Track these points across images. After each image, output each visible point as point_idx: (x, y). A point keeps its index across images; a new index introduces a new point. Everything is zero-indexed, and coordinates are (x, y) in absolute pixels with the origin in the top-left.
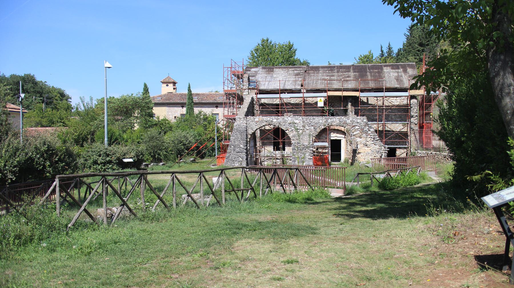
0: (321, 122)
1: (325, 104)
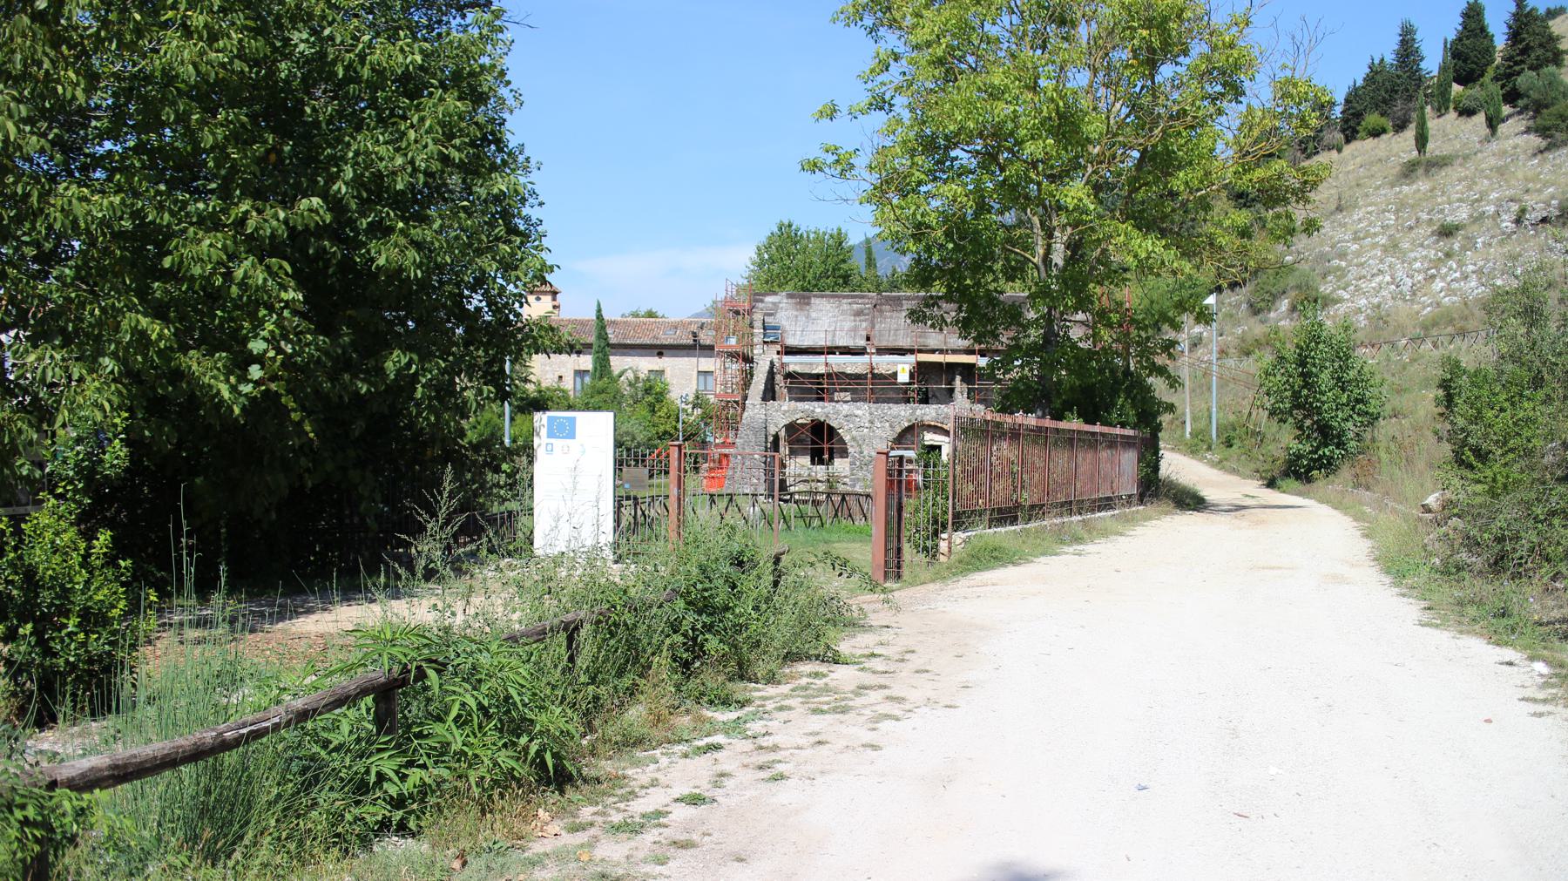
0: (904, 414)
1: (912, 375)
